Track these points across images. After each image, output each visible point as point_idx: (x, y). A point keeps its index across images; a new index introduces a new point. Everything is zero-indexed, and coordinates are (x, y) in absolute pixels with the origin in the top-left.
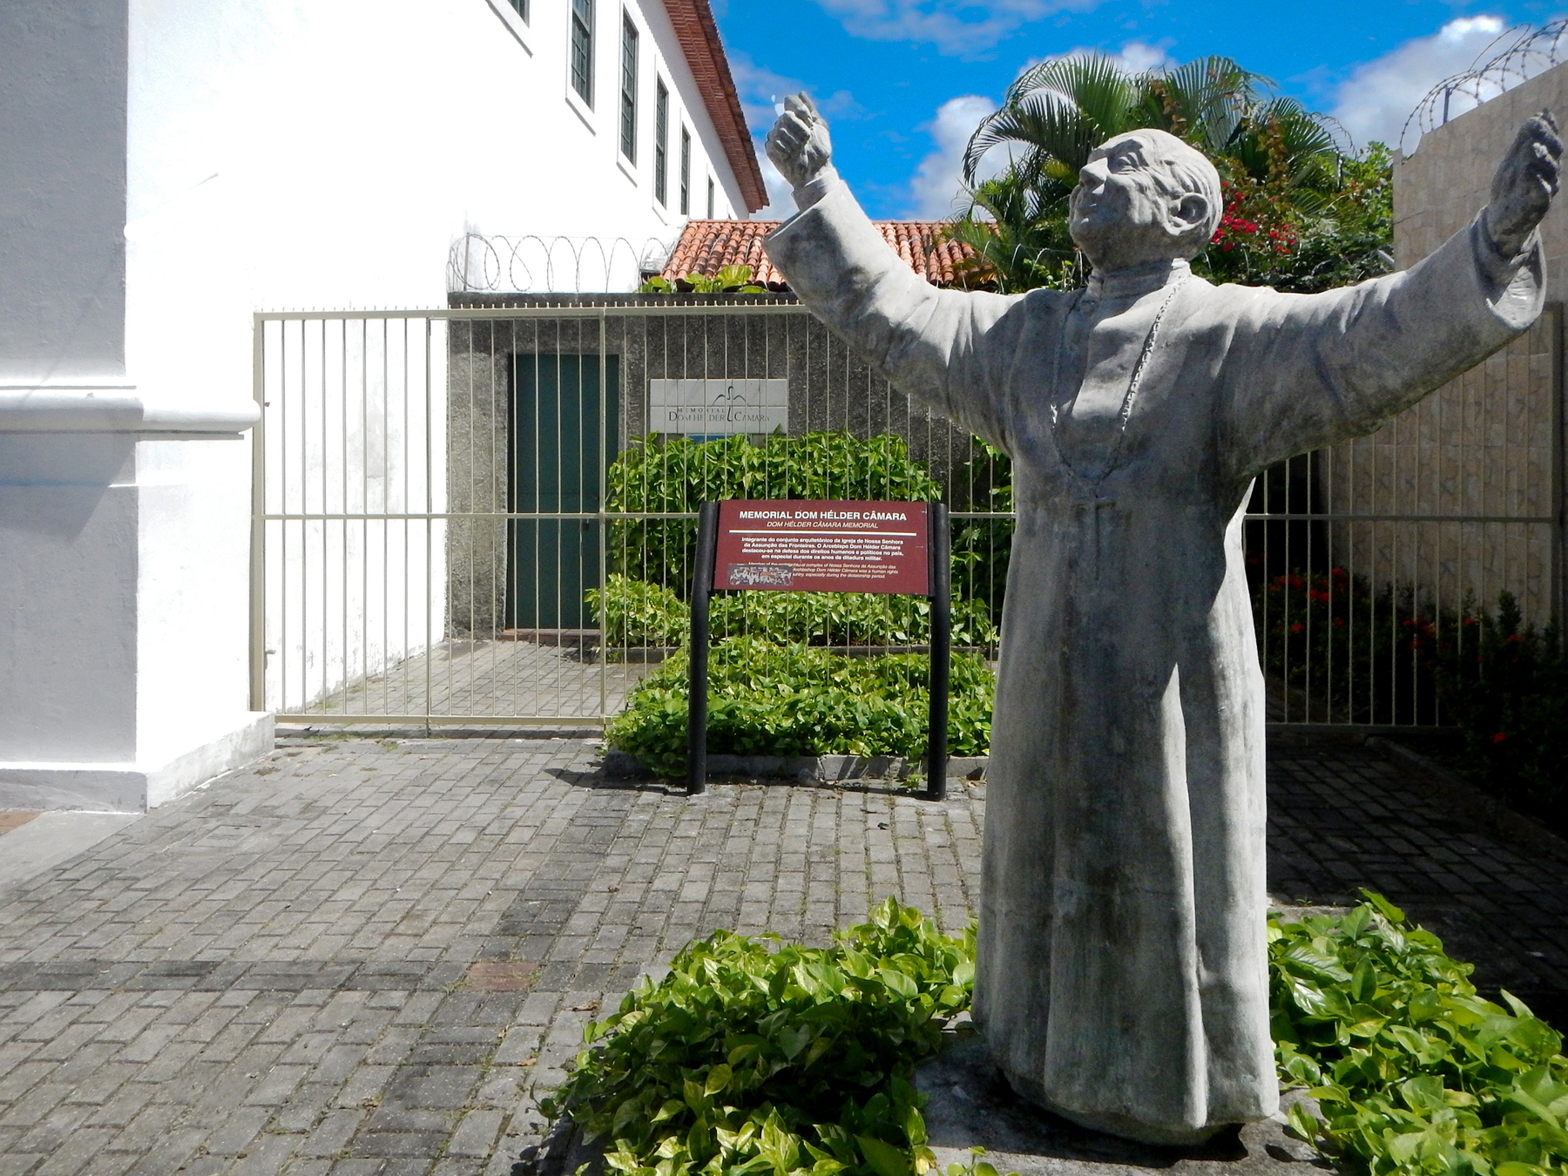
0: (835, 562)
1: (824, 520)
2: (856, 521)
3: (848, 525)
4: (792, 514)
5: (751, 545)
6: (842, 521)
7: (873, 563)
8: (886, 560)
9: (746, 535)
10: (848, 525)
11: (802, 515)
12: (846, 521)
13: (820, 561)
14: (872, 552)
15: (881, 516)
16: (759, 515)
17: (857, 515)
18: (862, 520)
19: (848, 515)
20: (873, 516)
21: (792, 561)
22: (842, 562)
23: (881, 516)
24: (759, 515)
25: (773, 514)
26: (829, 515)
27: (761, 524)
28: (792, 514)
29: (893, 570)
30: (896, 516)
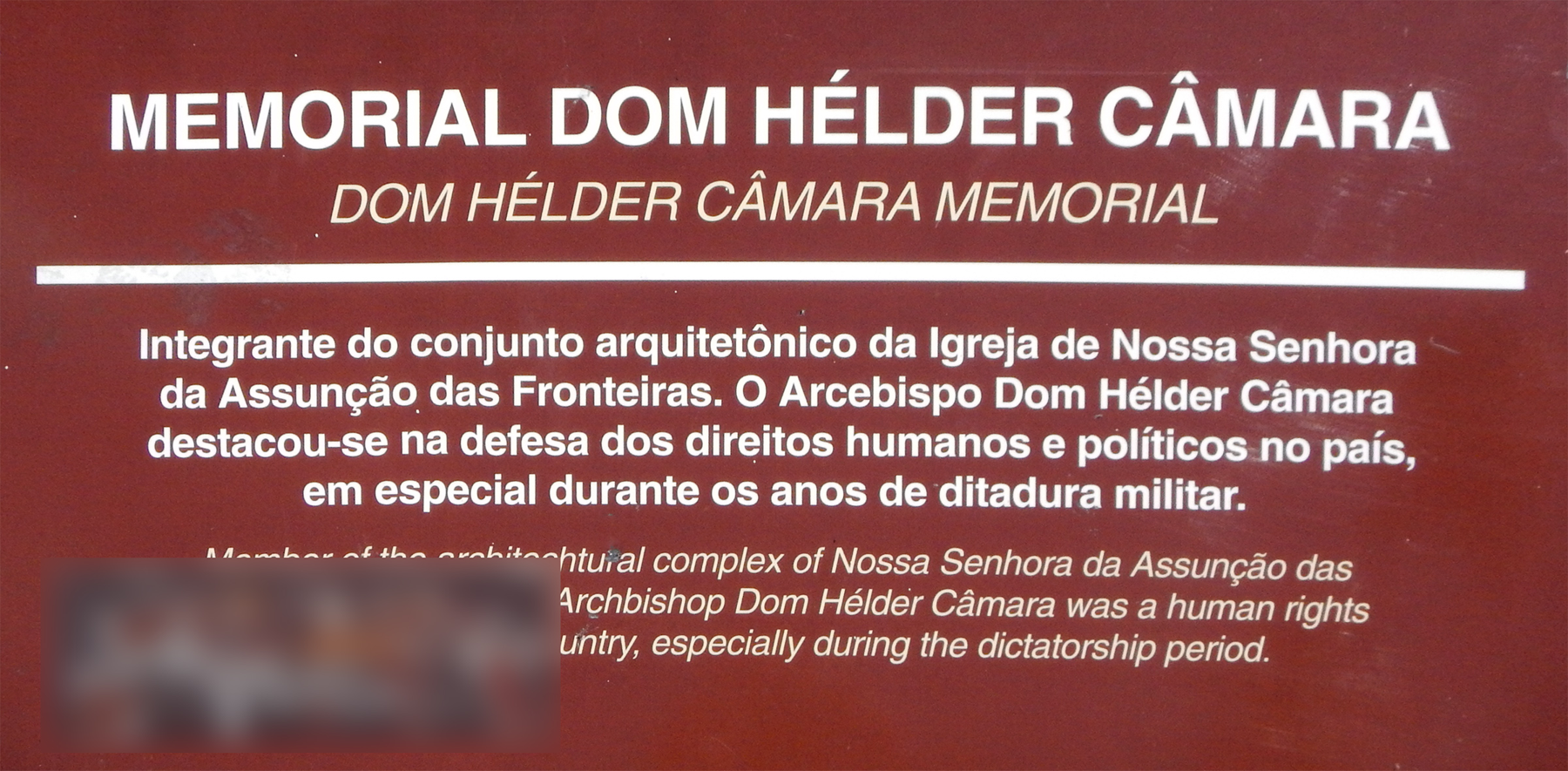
0: (875, 528)
1: (796, 162)
2: (1040, 163)
3: (980, 201)
4: (526, 111)
5: (212, 407)
6: (929, 168)
7: (1173, 532)
8: (1287, 510)
9: (169, 309)
10: (980, 201)
11: (604, 115)
12: (963, 162)
13: (759, 528)
14: (1168, 433)
15: (1247, 120)
16: (263, 121)
17: (1048, 110)
18: (1090, 158)
19: (976, 114)
20: (1183, 118)
21: (544, 526)
22: (932, 529)
23: (1247, 120)
24: (263, 121)
25: (372, 114)
26: (816, 112)
27: (273, 200)
28: (526, 111)
29: (1333, 597)
30: (1365, 114)
